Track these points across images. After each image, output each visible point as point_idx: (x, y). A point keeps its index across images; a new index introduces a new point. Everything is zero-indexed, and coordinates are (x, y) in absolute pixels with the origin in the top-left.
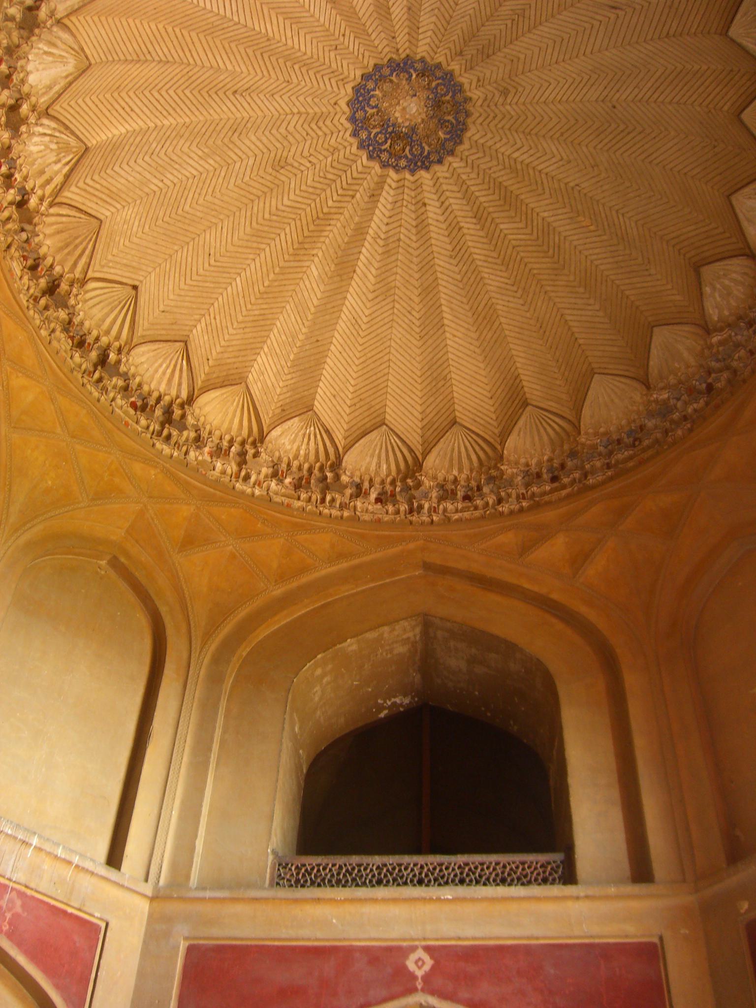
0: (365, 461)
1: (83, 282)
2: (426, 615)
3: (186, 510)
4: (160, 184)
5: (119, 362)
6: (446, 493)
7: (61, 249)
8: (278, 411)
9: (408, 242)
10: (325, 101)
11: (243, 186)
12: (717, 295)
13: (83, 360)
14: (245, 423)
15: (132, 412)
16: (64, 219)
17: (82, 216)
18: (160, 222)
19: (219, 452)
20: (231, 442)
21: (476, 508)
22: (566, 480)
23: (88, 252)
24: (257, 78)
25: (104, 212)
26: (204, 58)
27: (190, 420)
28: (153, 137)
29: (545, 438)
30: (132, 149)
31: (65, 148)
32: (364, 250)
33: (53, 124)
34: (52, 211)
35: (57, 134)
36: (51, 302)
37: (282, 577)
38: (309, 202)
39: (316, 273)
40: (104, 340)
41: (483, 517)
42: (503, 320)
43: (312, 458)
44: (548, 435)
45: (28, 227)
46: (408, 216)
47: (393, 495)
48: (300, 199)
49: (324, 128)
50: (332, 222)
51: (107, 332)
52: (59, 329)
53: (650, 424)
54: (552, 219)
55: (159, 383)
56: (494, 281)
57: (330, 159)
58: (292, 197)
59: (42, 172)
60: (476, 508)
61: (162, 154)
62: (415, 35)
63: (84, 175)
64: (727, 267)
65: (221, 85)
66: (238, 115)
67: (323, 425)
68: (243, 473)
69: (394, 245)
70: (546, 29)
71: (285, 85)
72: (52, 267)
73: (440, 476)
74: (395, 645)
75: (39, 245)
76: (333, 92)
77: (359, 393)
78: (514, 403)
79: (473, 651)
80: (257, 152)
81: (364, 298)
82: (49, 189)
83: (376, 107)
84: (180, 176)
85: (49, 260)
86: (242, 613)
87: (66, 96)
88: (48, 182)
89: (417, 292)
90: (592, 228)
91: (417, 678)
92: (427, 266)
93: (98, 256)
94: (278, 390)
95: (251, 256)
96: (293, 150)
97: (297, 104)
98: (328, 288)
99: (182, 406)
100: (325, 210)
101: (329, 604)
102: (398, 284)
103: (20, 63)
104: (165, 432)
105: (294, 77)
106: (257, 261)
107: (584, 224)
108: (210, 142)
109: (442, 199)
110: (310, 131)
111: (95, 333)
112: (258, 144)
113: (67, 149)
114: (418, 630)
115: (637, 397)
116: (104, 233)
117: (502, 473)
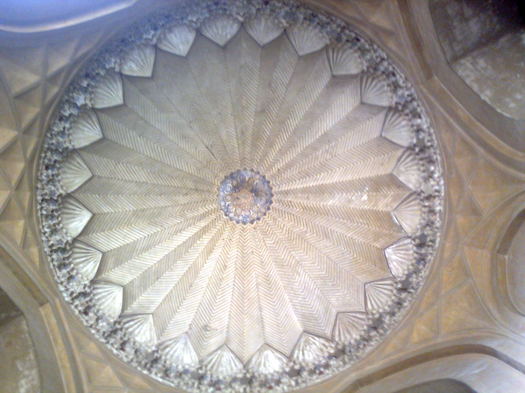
0: (403, 135)
1: (367, 313)
2: (448, 63)
3: (460, 220)
4: (317, 289)
5: (400, 282)
6: (395, 86)
7: (357, 328)
8: (401, 189)
9: (298, 168)
10: (255, 233)
11: (305, 251)
12: (228, 31)
13: (407, 300)
14: (413, 203)
15: (427, 265)
16: (341, 331)
17: (338, 322)
18: (335, 283)
19: (432, 211)
20: (425, 206)
21: (394, 68)
22: (353, 35)
23: (354, 315)
24: (256, 266)
25: (334, 312)
26: (254, 293)
27: (418, 234)
28: (296, 301)
29: (344, 56)
30: (304, 308)
31: (307, 342)
32: (311, 185)
33: (296, 352)
34: (337, 339)
35: (301, 348)
36: (380, 327)
37: (472, 151)
38: (301, 219)
39: (331, 201)
40: (395, 291)
41: (393, 62)
42: (307, 109)
43: (416, 161)
44: (341, 57)
45: (348, 349)
46: (288, 174)
47: (411, 112)
48: (302, 223)
49: (267, 228)
50: (306, 205)
51: (391, 291)
52: (394, 318)
53: (301, 17)
54: (252, 115)
55: (410, 255)
56: (293, 123)
57: (279, 219)
58: (302, 227)
59: (321, 350)
60: (394, 68)
61: (303, 294)
62: (210, 212)
63: (320, 328)
64: (213, 35)
65: (264, 280)
66: (274, 267)
67: (397, 164)
68: (437, 194)
69: (302, 173)
70: (178, 165)
71: (254, 253)
72: (364, 331)
73: (390, 94)
74: (479, 68)
75: (356, 340)
76: (250, 232)
77: (376, 154)
78: (338, 82)
79: (456, 23)
80: (288, 252)
81: (333, 174)
82: (327, 344)
83: (249, 211)
84: (310, 282)
85: (363, 333)
86: (501, 166)
87: (282, 350)
88: (324, 345)
89: (318, 153)
90: (245, 98)
91: (503, 41)
92: (304, 155)
93: (357, 309)
94: (392, 193)
95: (336, 234)
96: (281, 237)
97: (261, 244)
98: (335, 192)
99: (414, 240)
100: (302, 210)
101: (476, 118)
102: (318, 162)
103: (269, 377)
104: (430, 243)
105: (250, 251)
106: (336, 230)
107: (246, 102)
108: (291, 274)
109: (273, 164)
110: (271, 232)
111: (393, 298)
112: (284, 253)
113: (307, 342)
114: (463, 61)
115: (296, 30)
116: (344, 309)
117: (368, 68)
